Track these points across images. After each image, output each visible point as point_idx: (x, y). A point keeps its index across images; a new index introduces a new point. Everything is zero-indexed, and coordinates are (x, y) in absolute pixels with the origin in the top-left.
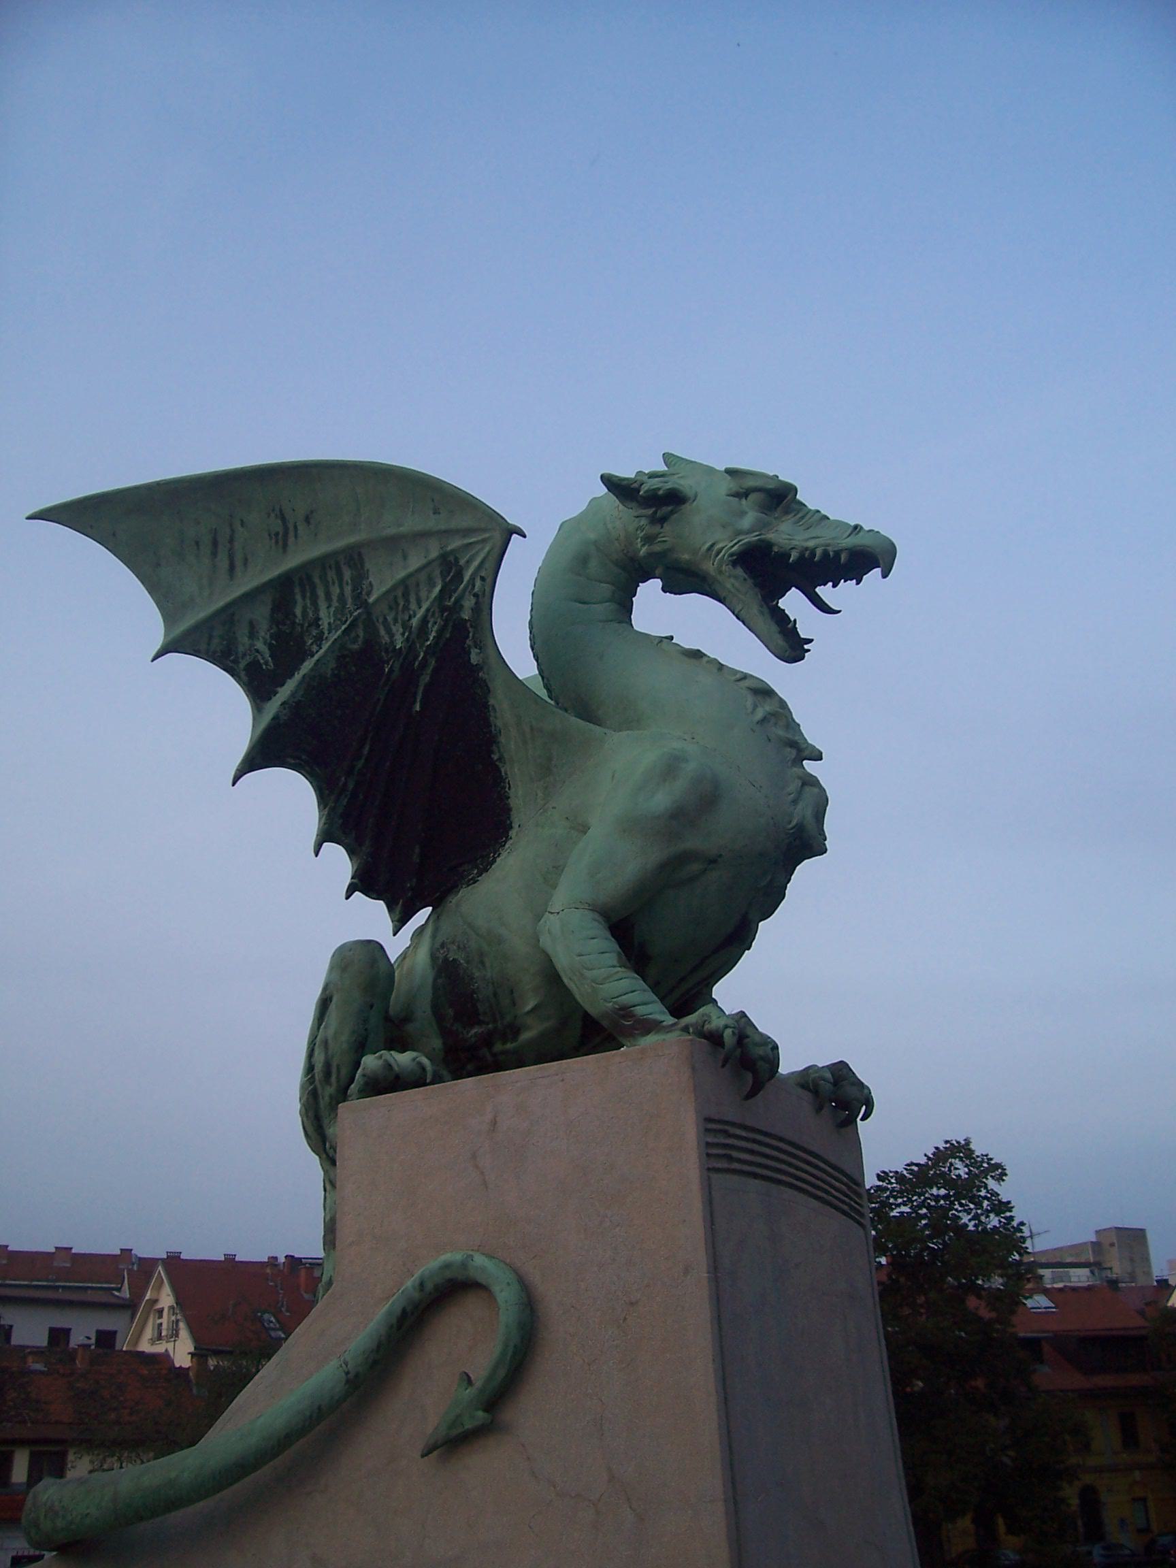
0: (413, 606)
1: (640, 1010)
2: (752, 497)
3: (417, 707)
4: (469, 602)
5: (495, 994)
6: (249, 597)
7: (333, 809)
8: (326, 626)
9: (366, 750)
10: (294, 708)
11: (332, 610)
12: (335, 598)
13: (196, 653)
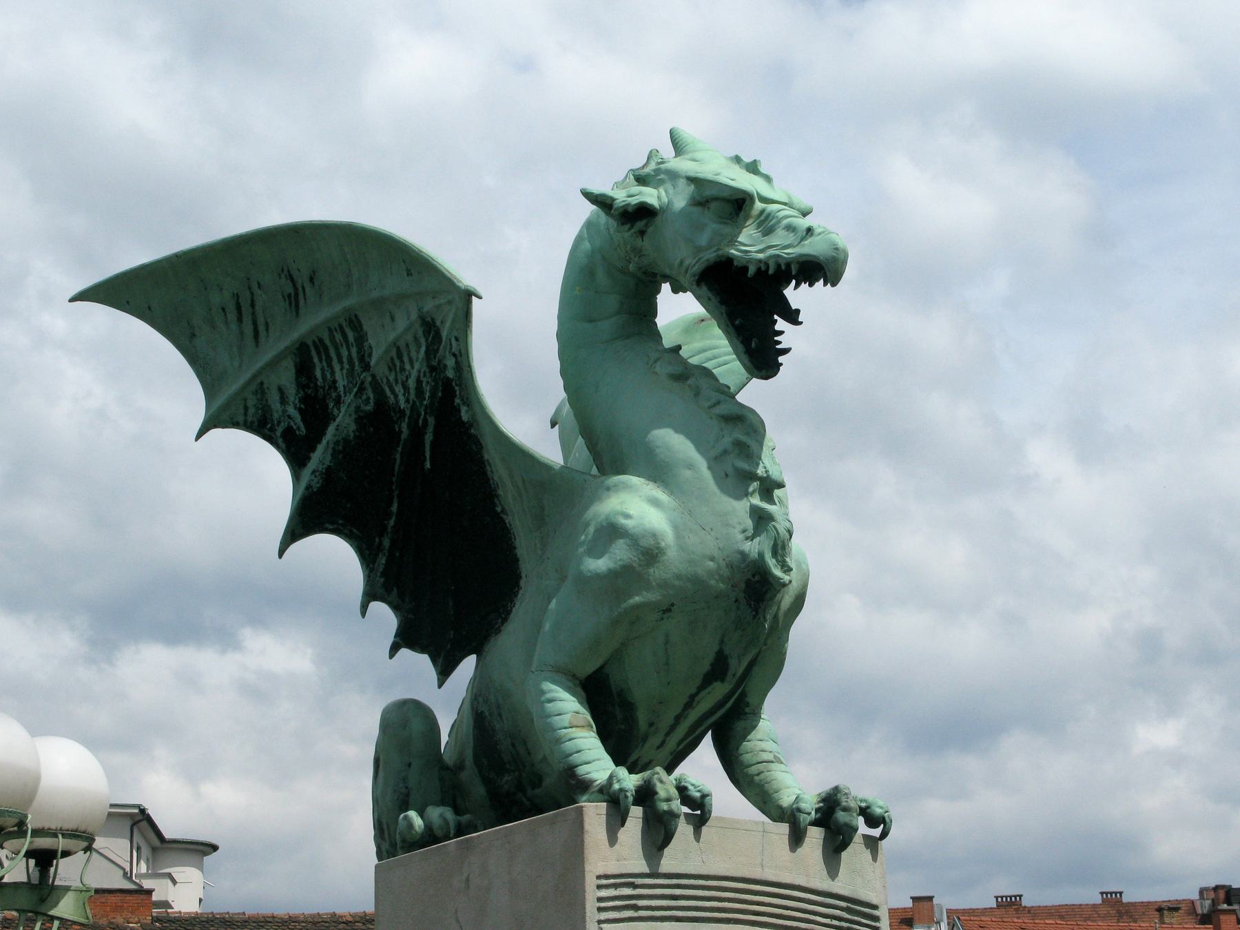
0: (408, 367)
2: (713, 205)
3: (428, 465)
4: (450, 362)
5: (513, 745)
6: (273, 364)
8: (341, 389)
9: (394, 508)
10: (328, 475)
12: (345, 360)
13: (235, 425)
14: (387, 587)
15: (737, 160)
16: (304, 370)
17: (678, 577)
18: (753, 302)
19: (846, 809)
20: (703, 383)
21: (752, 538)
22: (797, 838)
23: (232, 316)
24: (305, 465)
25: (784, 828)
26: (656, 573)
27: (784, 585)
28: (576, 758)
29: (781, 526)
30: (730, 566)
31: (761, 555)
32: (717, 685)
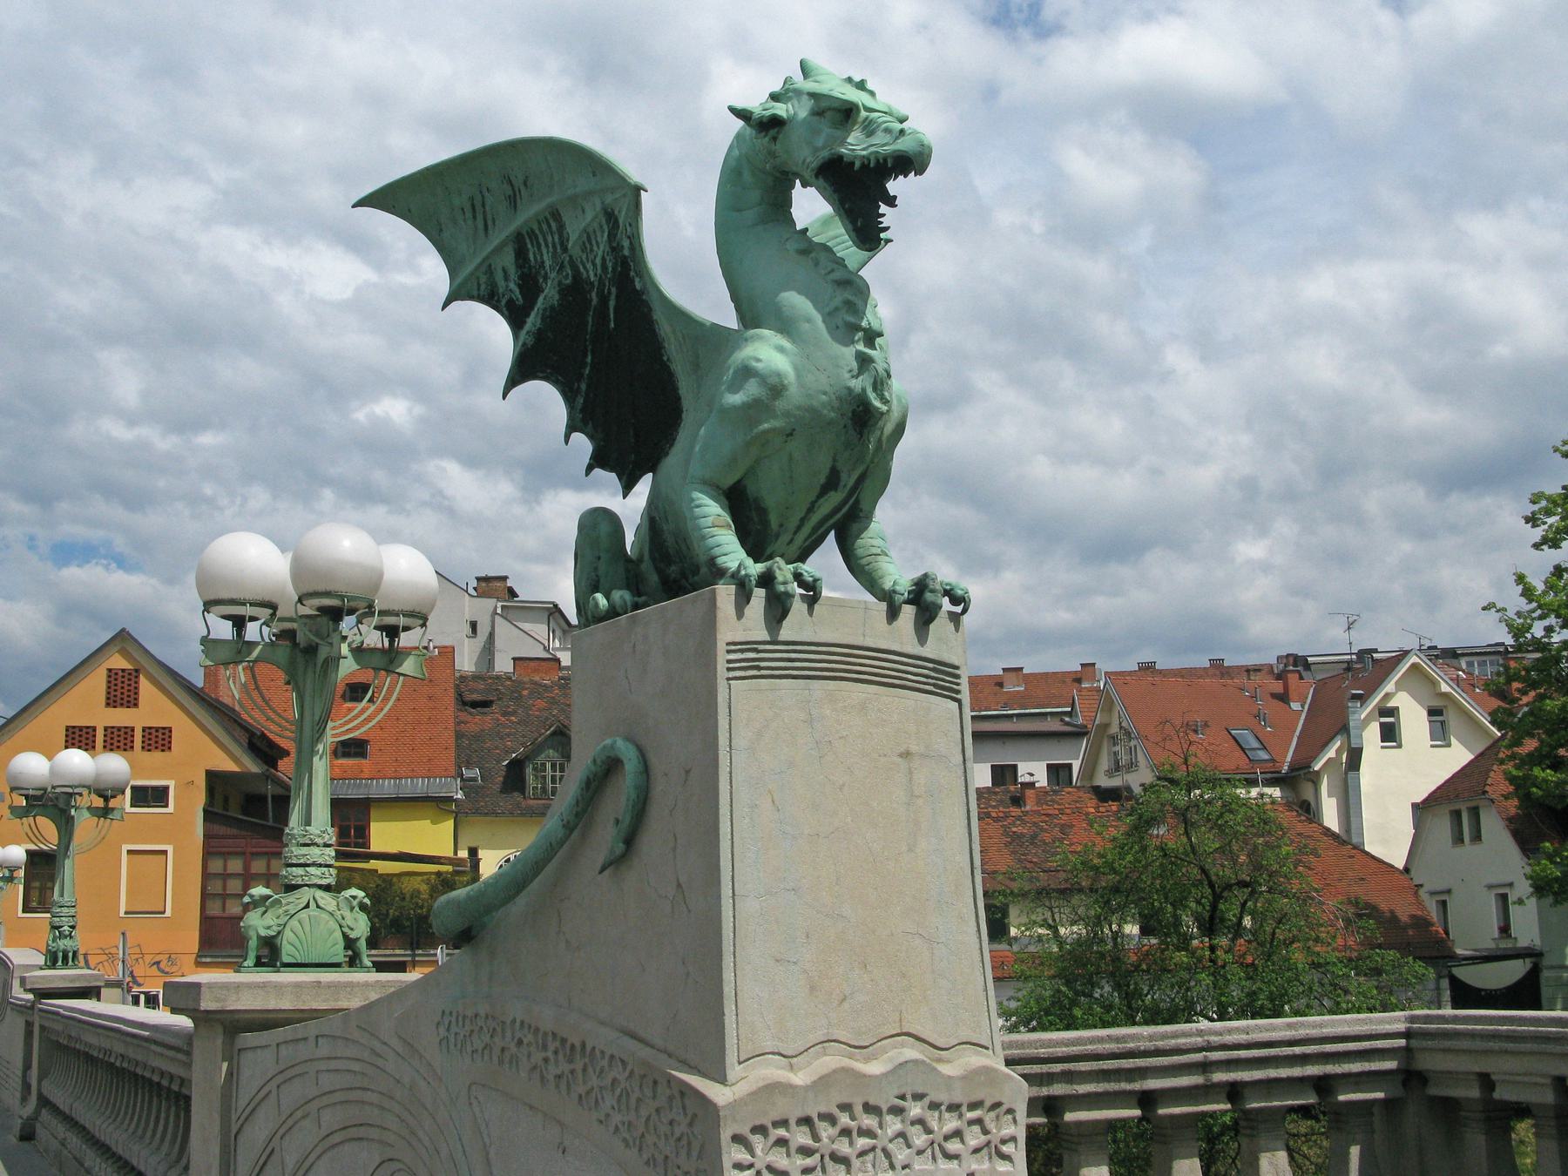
2: (829, 114)
4: (626, 243)
6: (498, 250)
10: (539, 335)
13: (471, 298)
14: (584, 421)
15: (849, 80)
16: (521, 254)
17: (799, 408)
18: (862, 189)
19: (932, 591)
20: (823, 256)
21: (857, 377)
22: (893, 614)
23: (469, 215)
25: (884, 606)
26: (780, 405)
27: (882, 414)
28: (717, 551)
29: (880, 366)
30: (839, 399)
31: (864, 390)
32: (832, 493)
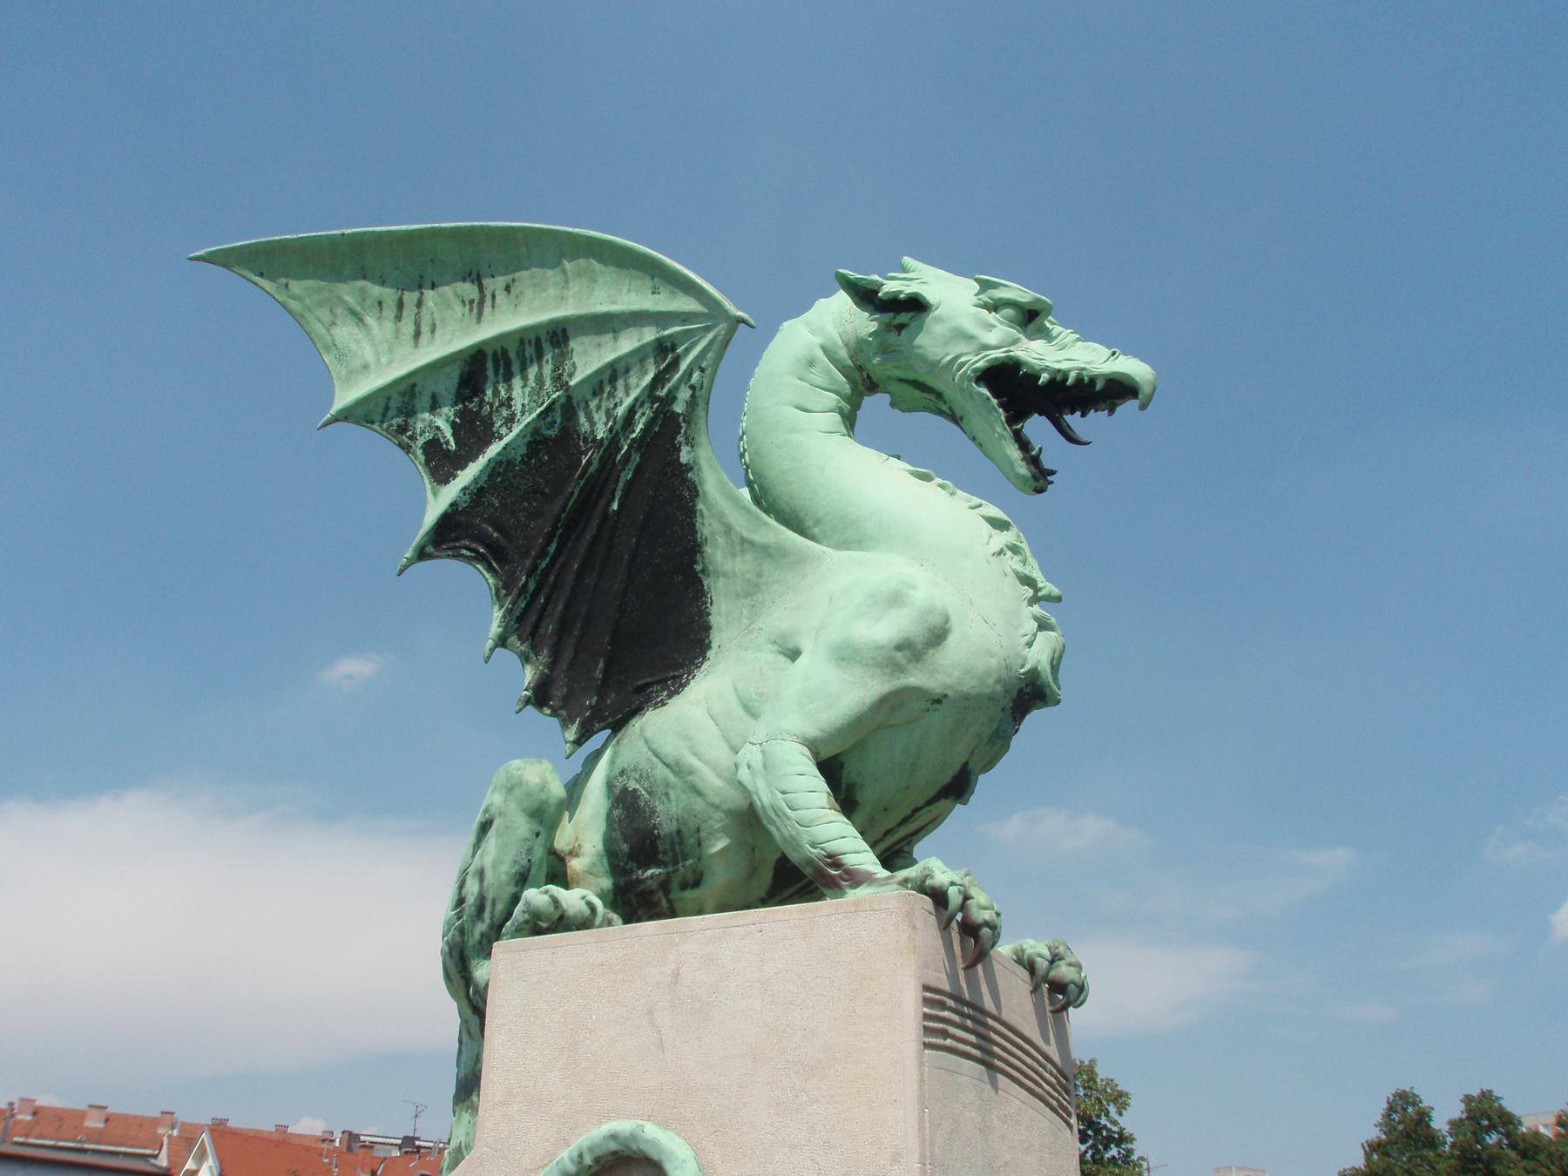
0: (620, 393)
1: (850, 860)
3: (615, 506)
4: (684, 394)
7: (509, 612)
8: (519, 407)
10: (477, 493)
11: (527, 390)
23: (389, 312)
24: (447, 482)
